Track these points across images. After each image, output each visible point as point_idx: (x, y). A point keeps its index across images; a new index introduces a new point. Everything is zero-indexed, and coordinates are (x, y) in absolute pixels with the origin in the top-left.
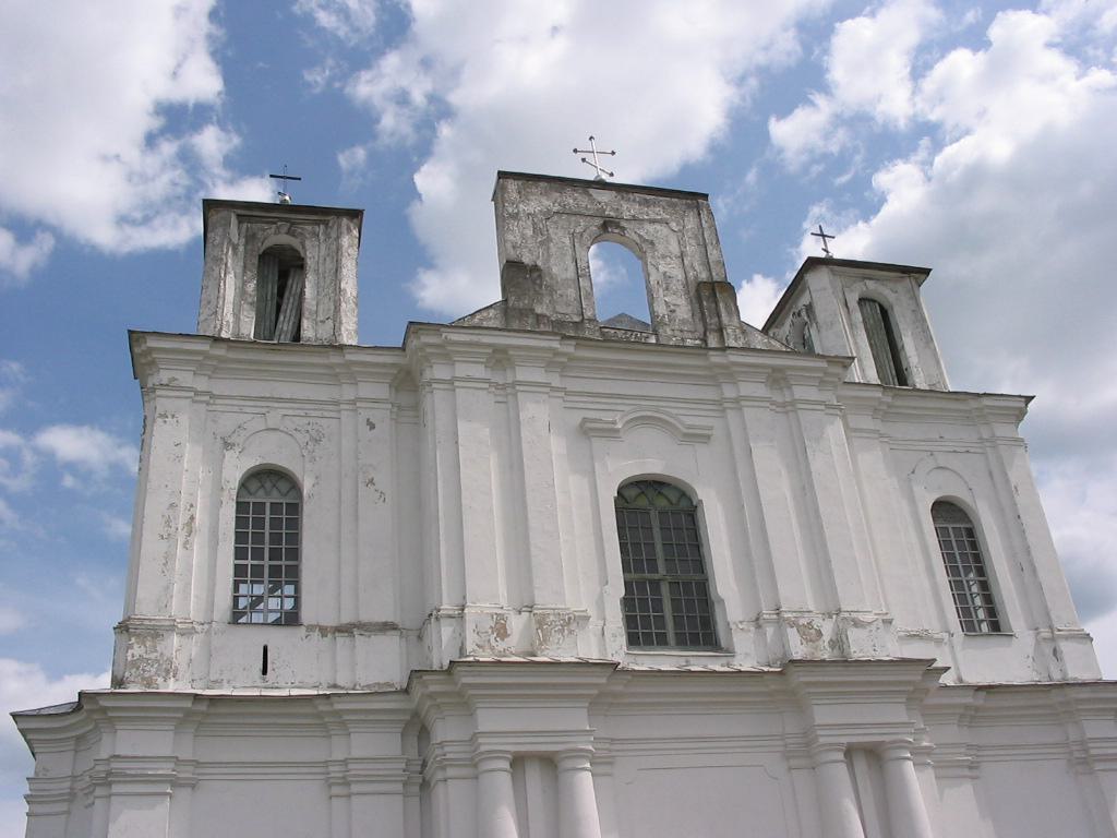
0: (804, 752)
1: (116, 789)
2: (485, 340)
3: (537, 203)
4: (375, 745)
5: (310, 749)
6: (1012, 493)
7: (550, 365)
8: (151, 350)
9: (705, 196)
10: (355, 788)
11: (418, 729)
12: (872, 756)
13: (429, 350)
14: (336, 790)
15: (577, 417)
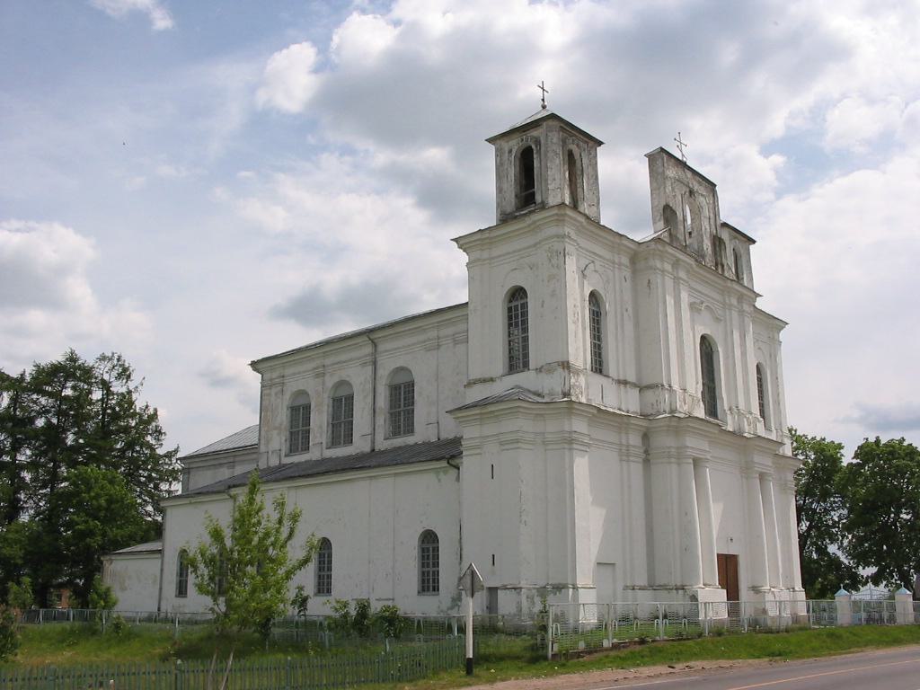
0: (746, 469)
1: (575, 446)
2: (678, 255)
3: (672, 172)
4: (635, 440)
5: (612, 436)
6: (776, 367)
7: (688, 272)
8: (566, 214)
9: (715, 186)
10: (631, 459)
11: (646, 437)
12: (762, 477)
13: (658, 252)
14: (624, 458)
15: (693, 300)
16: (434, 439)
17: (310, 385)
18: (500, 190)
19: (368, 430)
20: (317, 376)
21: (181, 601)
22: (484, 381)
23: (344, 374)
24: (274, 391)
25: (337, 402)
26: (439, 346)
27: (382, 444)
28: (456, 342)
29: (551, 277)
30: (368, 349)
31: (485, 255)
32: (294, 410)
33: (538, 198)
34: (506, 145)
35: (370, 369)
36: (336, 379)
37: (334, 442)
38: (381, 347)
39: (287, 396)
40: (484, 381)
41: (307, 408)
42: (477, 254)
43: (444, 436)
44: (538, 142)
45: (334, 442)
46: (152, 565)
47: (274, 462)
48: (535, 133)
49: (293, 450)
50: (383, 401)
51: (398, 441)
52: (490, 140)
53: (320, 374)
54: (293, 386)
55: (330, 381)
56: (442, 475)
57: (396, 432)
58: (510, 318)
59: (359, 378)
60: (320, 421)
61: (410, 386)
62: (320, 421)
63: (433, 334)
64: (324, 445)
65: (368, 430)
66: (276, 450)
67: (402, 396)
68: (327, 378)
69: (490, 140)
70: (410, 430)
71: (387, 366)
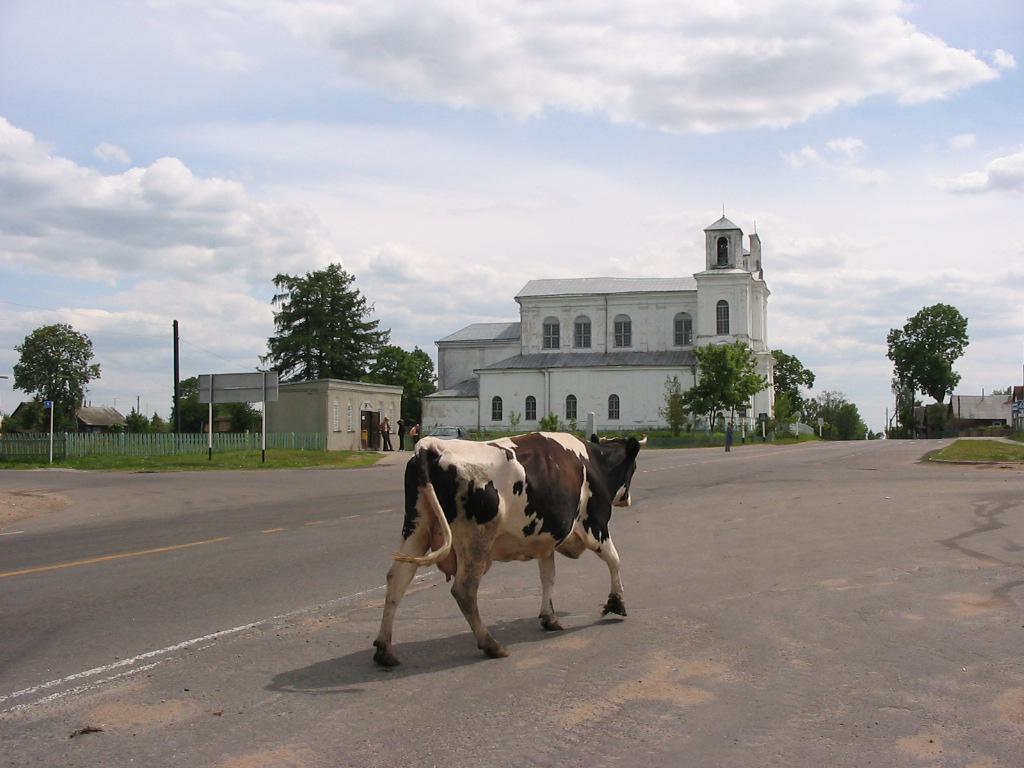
16: (645, 351)
17: (559, 315)
18: (709, 254)
19: (601, 340)
20: (566, 311)
21: (496, 422)
22: (707, 336)
23: (584, 312)
24: (531, 314)
25: (578, 326)
26: (647, 308)
27: (612, 349)
28: (657, 308)
29: (741, 300)
30: (602, 302)
31: (708, 284)
32: (546, 327)
33: (730, 263)
34: (713, 234)
35: (603, 312)
36: (579, 314)
37: (578, 344)
38: (610, 303)
39: (542, 319)
40: (707, 336)
41: (556, 328)
42: (702, 283)
43: (651, 350)
44: (730, 238)
45: (578, 344)
46: (471, 404)
47: (534, 352)
48: (728, 233)
49: (547, 345)
50: (611, 328)
51: (623, 349)
52: (705, 231)
53: (567, 309)
54: (546, 313)
55: (574, 314)
56: (685, 373)
57: (619, 343)
58: (718, 311)
59: (595, 317)
60: (567, 335)
61: (628, 326)
62: (567, 335)
63: (644, 301)
64: (572, 346)
65: (601, 340)
66: (534, 344)
67: (623, 331)
68: (572, 313)
69: (705, 231)
70: (628, 343)
71: (615, 312)
